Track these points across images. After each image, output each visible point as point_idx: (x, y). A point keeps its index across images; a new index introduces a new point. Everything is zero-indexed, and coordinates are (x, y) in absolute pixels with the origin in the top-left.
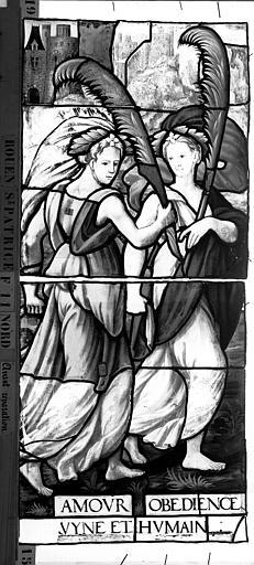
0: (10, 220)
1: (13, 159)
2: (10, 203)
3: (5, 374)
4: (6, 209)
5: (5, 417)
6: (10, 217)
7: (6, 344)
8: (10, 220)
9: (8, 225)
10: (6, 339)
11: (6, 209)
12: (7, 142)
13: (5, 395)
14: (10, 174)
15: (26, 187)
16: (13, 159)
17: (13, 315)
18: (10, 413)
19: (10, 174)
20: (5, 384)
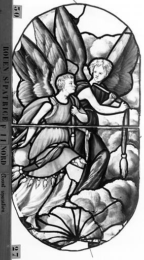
0: (6, 92)
1: (8, 58)
2: (6, 82)
3: (3, 181)
4: (4, 86)
5: (3, 204)
6: (6, 90)
7: (4, 163)
8: (6, 92)
9: (5, 95)
10: (4, 160)
11: (4, 86)
12: (4, 48)
13: (2, 192)
14: (6, 66)
15: (14, 166)
16: (8, 58)
17: (8, 147)
18: (6, 202)
19: (6, 66)
20: (3, 185)
